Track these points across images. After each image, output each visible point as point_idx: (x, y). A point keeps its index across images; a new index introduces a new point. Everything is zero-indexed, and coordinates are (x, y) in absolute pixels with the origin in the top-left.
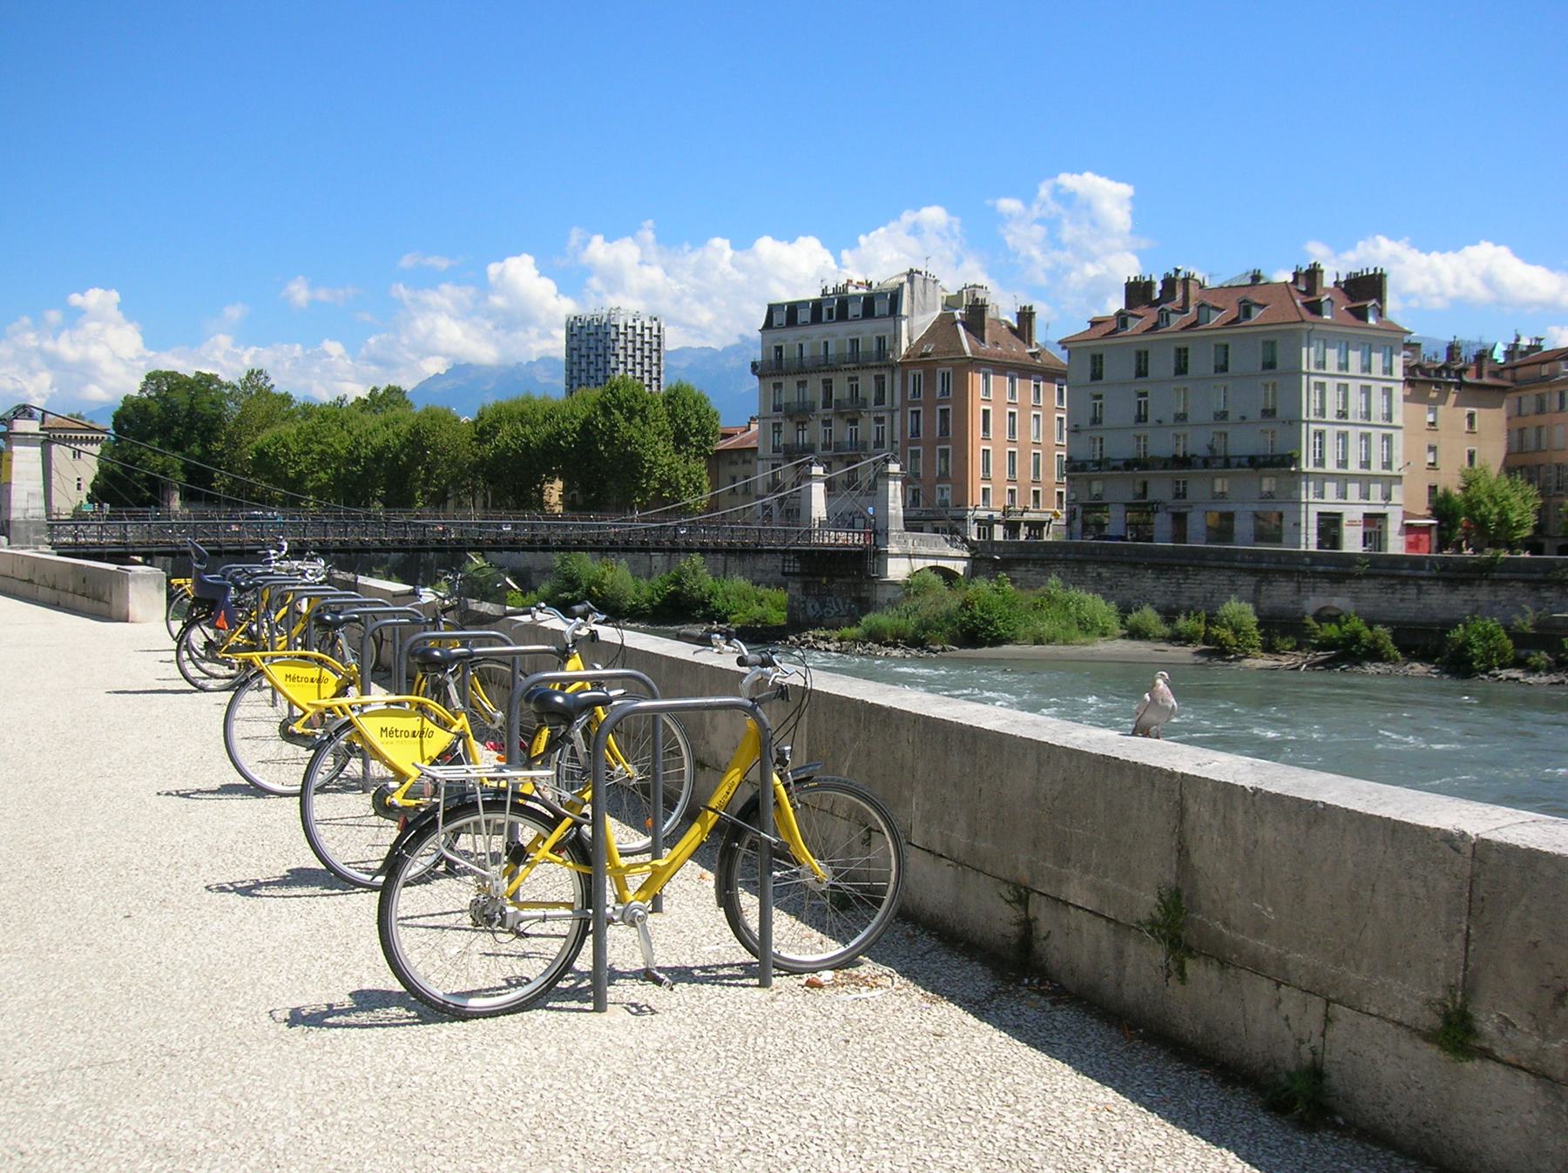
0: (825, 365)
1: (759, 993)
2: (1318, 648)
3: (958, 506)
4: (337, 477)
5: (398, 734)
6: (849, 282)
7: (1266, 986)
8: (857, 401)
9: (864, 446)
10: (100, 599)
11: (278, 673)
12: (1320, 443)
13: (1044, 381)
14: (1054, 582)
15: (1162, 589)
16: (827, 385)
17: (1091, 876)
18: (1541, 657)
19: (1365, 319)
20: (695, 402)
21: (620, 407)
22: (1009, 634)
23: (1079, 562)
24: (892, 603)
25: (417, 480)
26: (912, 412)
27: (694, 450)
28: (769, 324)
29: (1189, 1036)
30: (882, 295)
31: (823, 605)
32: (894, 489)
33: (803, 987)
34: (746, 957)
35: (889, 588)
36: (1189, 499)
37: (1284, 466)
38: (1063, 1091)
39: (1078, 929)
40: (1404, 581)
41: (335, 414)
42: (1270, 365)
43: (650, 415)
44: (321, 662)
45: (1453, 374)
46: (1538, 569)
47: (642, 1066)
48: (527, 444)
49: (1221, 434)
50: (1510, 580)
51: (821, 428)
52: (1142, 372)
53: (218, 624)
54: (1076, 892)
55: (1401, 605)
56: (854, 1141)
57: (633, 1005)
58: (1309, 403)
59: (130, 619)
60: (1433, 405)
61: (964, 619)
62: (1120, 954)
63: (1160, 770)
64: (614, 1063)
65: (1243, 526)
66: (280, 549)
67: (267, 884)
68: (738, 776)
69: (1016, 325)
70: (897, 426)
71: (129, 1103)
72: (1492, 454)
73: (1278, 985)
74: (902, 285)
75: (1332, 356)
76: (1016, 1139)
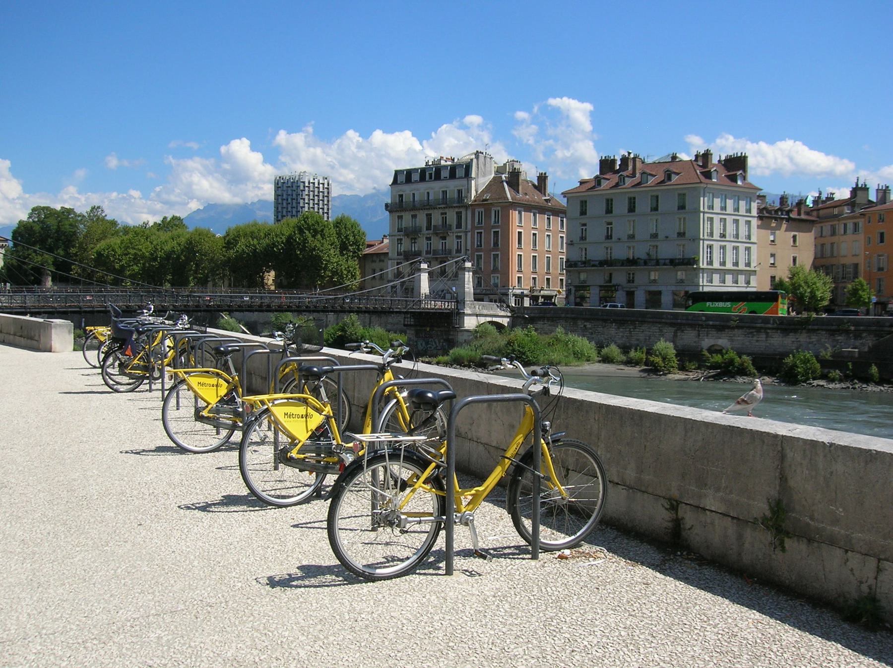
0: (427, 205)
1: (533, 563)
2: (710, 368)
3: (504, 287)
4: (143, 268)
5: (294, 416)
6: (442, 158)
7: (839, 553)
8: (446, 226)
9: (450, 252)
10: (32, 338)
11: (193, 381)
12: (710, 252)
13: (552, 215)
14: (559, 330)
15: (621, 334)
16: (429, 217)
17: (721, 494)
18: (836, 373)
19: (736, 182)
20: (352, 227)
21: (309, 229)
22: (534, 360)
23: (574, 319)
24: (467, 342)
25: (191, 270)
26: (478, 233)
27: (351, 254)
28: (395, 182)
29: (787, 581)
30: (461, 165)
31: (427, 343)
32: (468, 277)
33: (556, 559)
34: (523, 542)
35: (466, 334)
36: (636, 284)
37: (690, 265)
38: (731, 613)
39: (712, 523)
40: (759, 330)
41: (142, 232)
42: (682, 207)
43: (326, 234)
44: (218, 375)
45: (784, 213)
46: (834, 324)
47: (490, 605)
48: (255, 250)
49: (654, 246)
50: (818, 330)
51: (425, 242)
52: (609, 211)
53: (127, 353)
54: (711, 502)
55: (757, 344)
56: (631, 643)
57: (466, 571)
58: (704, 229)
59: (53, 350)
60: (773, 230)
61: (508, 351)
62: (740, 537)
63: (768, 434)
64: (474, 604)
65: (666, 299)
66: (149, 309)
67: (214, 504)
68: (522, 439)
69: (537, 184)
70: (469, 241)
71: (200, 635)
72: (806, 259)
73: (847, 551)
74: (472, 160)
75: (717, 202)
76: (719, 640)
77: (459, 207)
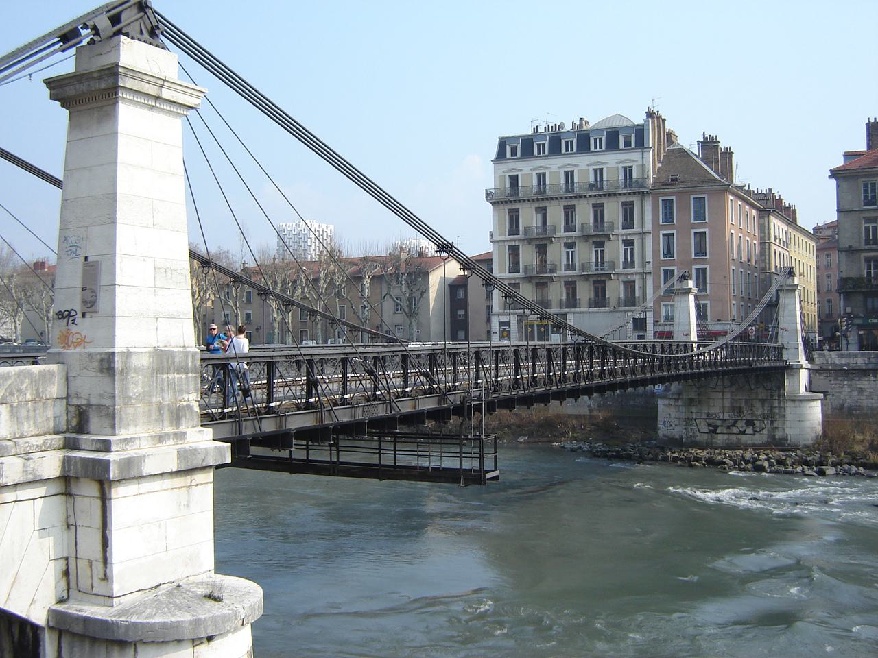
0: (569, 192)
3: (719, 320)
26: (664, 235)
28: (501, 155)
77: (629, 194)
